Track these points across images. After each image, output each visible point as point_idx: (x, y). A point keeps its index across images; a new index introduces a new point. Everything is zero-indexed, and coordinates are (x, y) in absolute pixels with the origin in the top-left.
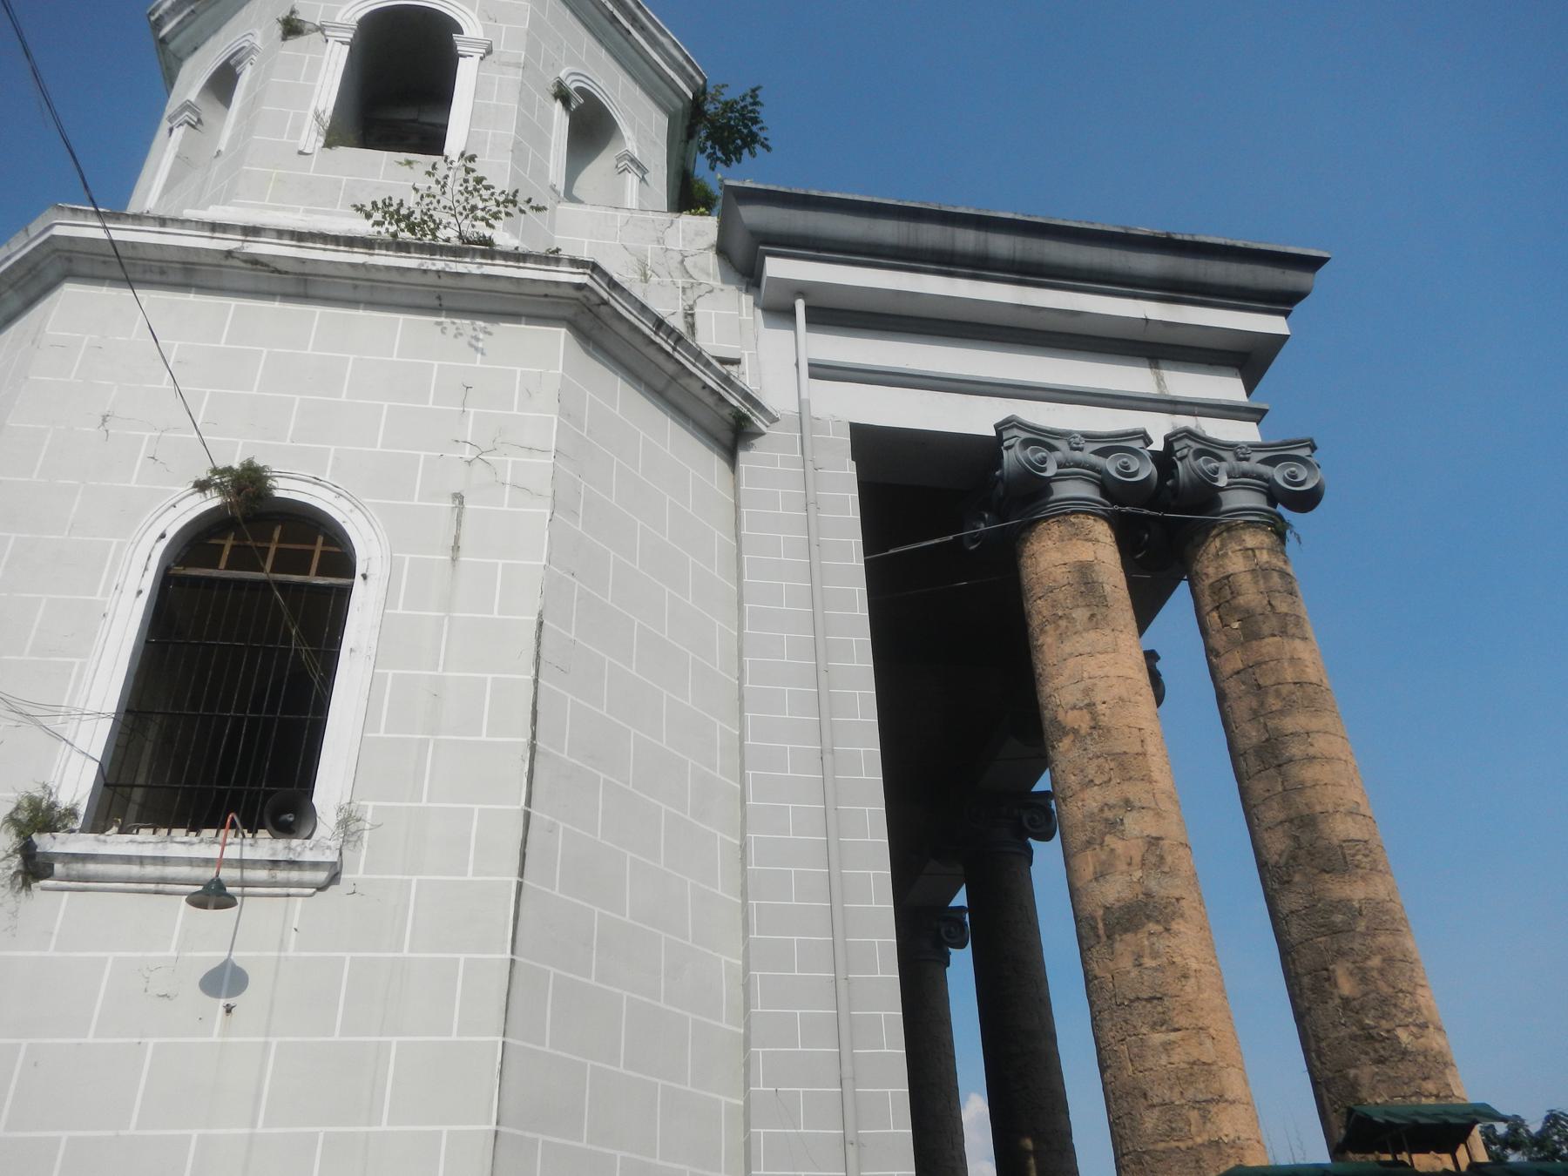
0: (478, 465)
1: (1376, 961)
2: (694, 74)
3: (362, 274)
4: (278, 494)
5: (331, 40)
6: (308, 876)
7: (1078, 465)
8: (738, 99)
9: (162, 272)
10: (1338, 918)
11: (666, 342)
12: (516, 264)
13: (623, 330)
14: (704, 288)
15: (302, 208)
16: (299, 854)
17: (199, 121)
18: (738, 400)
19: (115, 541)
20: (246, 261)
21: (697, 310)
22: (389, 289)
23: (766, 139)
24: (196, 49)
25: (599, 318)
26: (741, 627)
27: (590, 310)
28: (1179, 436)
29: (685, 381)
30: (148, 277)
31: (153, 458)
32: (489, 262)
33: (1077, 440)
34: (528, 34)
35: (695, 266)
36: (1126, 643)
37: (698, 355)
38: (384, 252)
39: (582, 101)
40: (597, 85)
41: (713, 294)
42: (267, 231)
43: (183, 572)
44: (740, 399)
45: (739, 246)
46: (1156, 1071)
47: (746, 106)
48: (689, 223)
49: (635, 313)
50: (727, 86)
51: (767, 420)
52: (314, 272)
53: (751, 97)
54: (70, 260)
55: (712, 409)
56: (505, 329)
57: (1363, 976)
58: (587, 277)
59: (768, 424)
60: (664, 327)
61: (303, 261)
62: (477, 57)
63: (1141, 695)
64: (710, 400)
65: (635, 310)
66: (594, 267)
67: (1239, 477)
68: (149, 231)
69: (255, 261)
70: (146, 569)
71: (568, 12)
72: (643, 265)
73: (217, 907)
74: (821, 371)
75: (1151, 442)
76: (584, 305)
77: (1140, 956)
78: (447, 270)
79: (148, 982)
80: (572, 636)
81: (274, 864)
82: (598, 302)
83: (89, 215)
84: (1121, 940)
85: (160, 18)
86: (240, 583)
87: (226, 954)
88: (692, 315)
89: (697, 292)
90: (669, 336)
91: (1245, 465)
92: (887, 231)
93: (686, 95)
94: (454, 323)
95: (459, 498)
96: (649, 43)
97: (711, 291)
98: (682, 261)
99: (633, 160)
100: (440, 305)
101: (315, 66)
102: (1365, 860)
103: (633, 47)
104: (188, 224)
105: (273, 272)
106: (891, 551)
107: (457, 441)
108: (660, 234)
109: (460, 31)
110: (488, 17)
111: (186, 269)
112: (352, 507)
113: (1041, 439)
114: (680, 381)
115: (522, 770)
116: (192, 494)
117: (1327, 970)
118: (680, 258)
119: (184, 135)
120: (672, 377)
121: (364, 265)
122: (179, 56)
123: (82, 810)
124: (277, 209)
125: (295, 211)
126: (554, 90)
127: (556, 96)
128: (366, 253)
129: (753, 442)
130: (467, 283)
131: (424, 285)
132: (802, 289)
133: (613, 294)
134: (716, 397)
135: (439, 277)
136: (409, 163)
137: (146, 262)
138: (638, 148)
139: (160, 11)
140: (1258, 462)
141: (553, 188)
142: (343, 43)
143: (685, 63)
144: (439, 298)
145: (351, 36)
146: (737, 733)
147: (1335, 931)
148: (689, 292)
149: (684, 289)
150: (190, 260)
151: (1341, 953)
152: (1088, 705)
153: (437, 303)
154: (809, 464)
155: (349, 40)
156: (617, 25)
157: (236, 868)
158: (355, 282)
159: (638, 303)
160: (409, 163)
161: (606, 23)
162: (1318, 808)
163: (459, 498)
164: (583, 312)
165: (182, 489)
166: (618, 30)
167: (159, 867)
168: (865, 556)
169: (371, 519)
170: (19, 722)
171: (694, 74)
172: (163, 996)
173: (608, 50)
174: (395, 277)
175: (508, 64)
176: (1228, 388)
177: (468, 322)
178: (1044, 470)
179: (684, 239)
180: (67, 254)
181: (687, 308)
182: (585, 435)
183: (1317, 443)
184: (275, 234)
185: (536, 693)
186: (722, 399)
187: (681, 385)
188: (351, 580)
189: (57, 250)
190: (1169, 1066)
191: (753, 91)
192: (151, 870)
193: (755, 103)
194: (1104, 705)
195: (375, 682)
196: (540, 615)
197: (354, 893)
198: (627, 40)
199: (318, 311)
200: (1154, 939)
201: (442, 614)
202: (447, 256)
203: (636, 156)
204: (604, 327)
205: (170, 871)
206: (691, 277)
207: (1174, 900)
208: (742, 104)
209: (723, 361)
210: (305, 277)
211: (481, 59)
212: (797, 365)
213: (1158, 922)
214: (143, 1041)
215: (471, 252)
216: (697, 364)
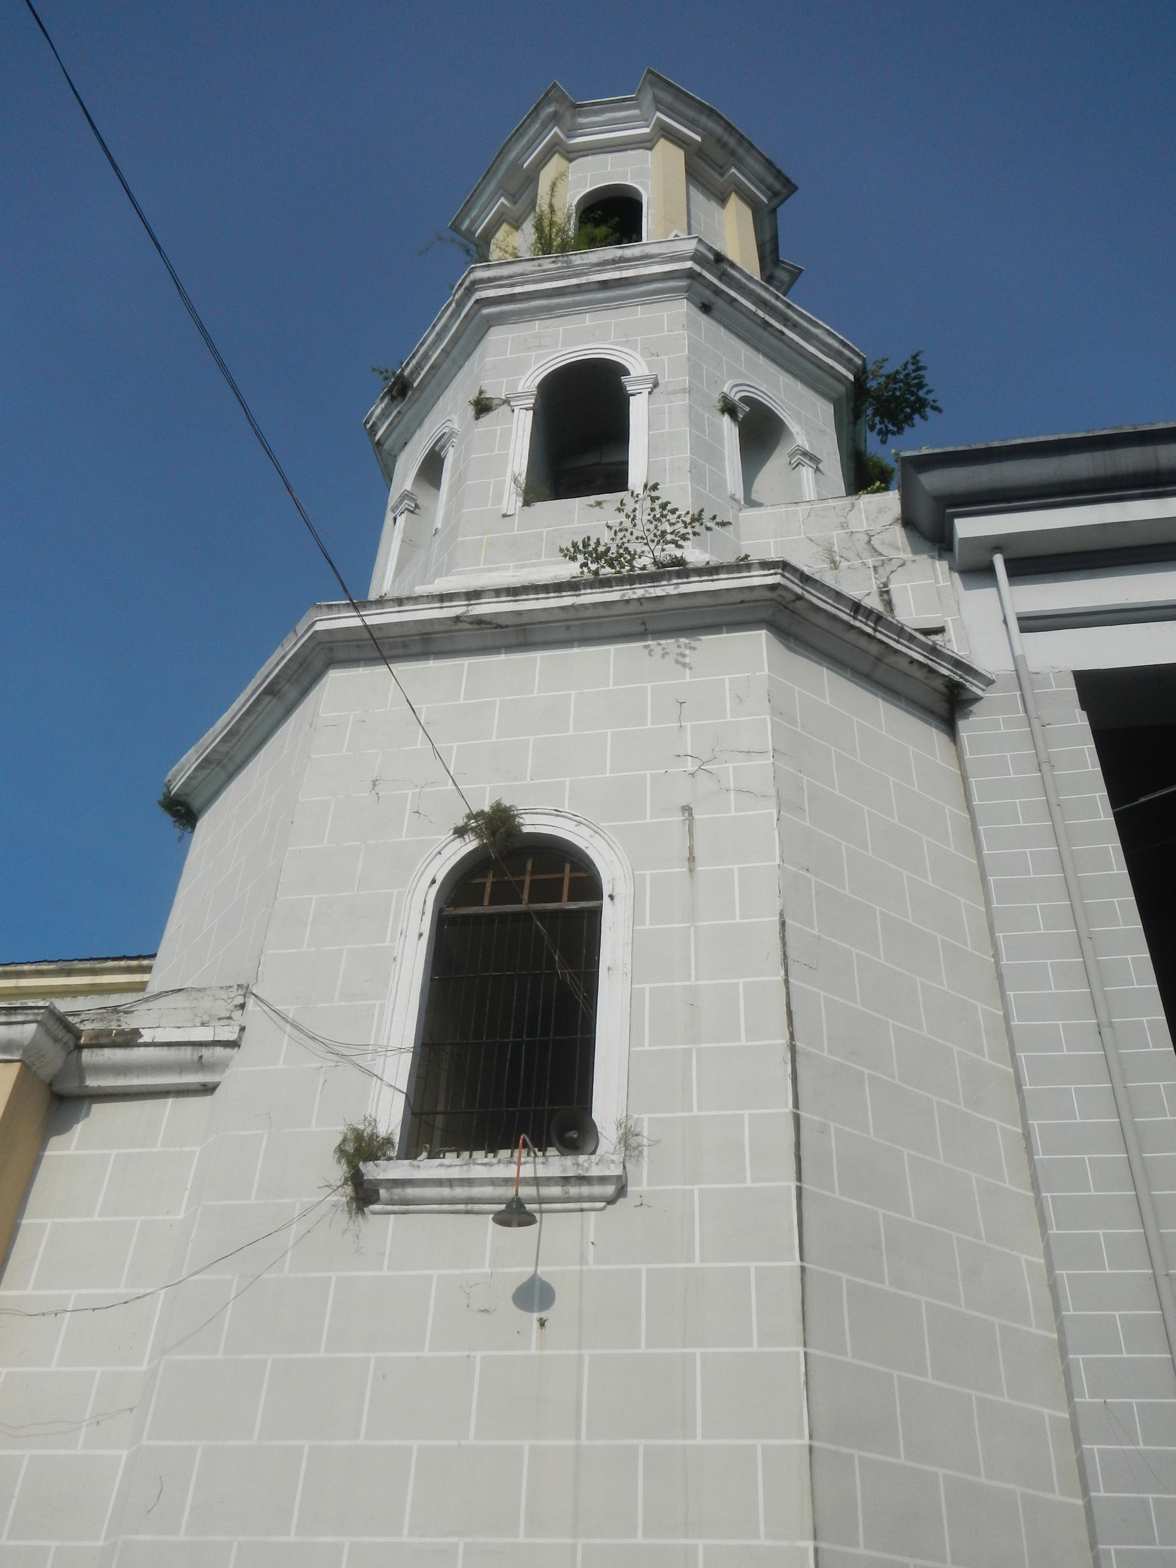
0: (701, 776)
2: (852, 356)
3: (572, 615)
4: (526, 829)
5: (516, 409)
6: (597, 1190)
8: (900, 369)
9: (405, 646)
11: (866, 624)
12: (711, 578)
13: (820, 620)
14: (895, 563)
15: (512, 565)
16: (587, 1169)
17: (417, 506)
18: (948, 669)
19: (395, 891)
20: (471, 623)
21: (891, 586)
23: (934, 401)
24: (406, 444)
25: (798, 614)
26: (988, 902)
27: (786, 608)
29: (891, 659)
30: (394, 652)
31: (417, 812)
32: (685, 580)
34: (689, 361)
35: (883, 543)
37: (900, 631)
38: (589, 591)
39: (747, 409)
40: (760, 391)
41: (905, 567)
42: (486, 593)
43: (453, 912)
44: (950, 667)
45: (924, 516)
47: (908, 375)
48: (869, 502)
49: (831, 602)
50: (887, 360)
51: (982, 684)
52: (530, 621)
53: (913, 364)
54: (331, 649)
55: (923, 683)
56: (708, 640)
58: (779, 576)
59: (984, 687)
60: (861, 611)
61: (519, 613)
62: (646, 392)
64: (920, 674)
66: (785, 566)
68: (390, 612)
69: (480, 622)
70: (423, 913)
71: (722, 329)
72: (830, 552)
73: (520, 1225)
74: (1032, 623)
76: (780, 604)
78: (647, 595)
79: (469, 1298)
80: (816, 932)
81: (566, 1180)
82: (793, 598)
83: (342, 608)
85: (374, 423)
86: (503, 917)
87: (532, 1269)
88: (888, 592)
89: (889, 568)
90: (867, 618)
92: (1080, 465)
93: (846, 378)
94: (660, 644)
95: (687, 810)
97: (902, 565)
98: (869, 542)
99: (805, 454)
100: (646, 630)
101: (507, 434)
103: (788, 345)
104: (420, 599)
105: (496, 628)
106: (1142, 800)
108: (843, 520)
109: (627, 373)
110: (650, 352)
114: (884, 660)
115: (786, 1072)
116: (453, 840)
118: (866, 538)
119: (406, 521)
121: (572, 606)
122: (393, 453)
123: (396, 1139)
124: (491, 570)
125: (507, 568)
126: (719, 405)
127: (723, 411)
128: (573, 595)
129: (971, 708)
130: (668, 604)
132: (998, 544)
133: (807, 588)
134: (925, 670)
135: (641, 604)
136: (599, 504)
137: (391, 640)
138: (808, 440)
139: (374, 419)
141: (733, 498)
142: (527, 409)
143: (841, 348)
144: (644, 623)
145: (533, 401)
146: (1001, 1014)
148: (880, 570)
149: (875, 568)
150: (426, 631)
153: (642, 628)
154: (1036, 724)
155: (532, 405)
156: (770, 329)
157: (533, 1186)
158: (566, 623)
160: (599, 504)
161: (759, 330)
164: (780, 611)
165: (443, 837)
166: (772, 334)
167: (467, 1189)
168: (1113, 808)
169: (610, 842)
170: (337, 1062)
171: (852, 356)
172: (483, 1311)
173: (766, 355)
174: (602, 612)
175: (675, 392)
177: (672, 641)
179: (867, 519)
180: (329, 645)
181: (881, 586)
182: (799, 730)
184: (493, 593)
185: (788, 994)
186: (932, 671)
188: (599, 902)
191: (914, 357)
192: (460, 1192)
193: (918, 369)
195: (634, 998)
196: (781, 915)
197: (642, 1204)
198: (782, 341)
199: (538, 657)
201: (688, 925)
202: (645, 583)
203: (807, 448)
205: (477, 1191)
206: (881, 554)
208: (904, 373)
209: (927, 632)
211: (650, 393)
212: (1005, 622)
214: (472, 1354)
215: (667, 576)
216: (901, 640)
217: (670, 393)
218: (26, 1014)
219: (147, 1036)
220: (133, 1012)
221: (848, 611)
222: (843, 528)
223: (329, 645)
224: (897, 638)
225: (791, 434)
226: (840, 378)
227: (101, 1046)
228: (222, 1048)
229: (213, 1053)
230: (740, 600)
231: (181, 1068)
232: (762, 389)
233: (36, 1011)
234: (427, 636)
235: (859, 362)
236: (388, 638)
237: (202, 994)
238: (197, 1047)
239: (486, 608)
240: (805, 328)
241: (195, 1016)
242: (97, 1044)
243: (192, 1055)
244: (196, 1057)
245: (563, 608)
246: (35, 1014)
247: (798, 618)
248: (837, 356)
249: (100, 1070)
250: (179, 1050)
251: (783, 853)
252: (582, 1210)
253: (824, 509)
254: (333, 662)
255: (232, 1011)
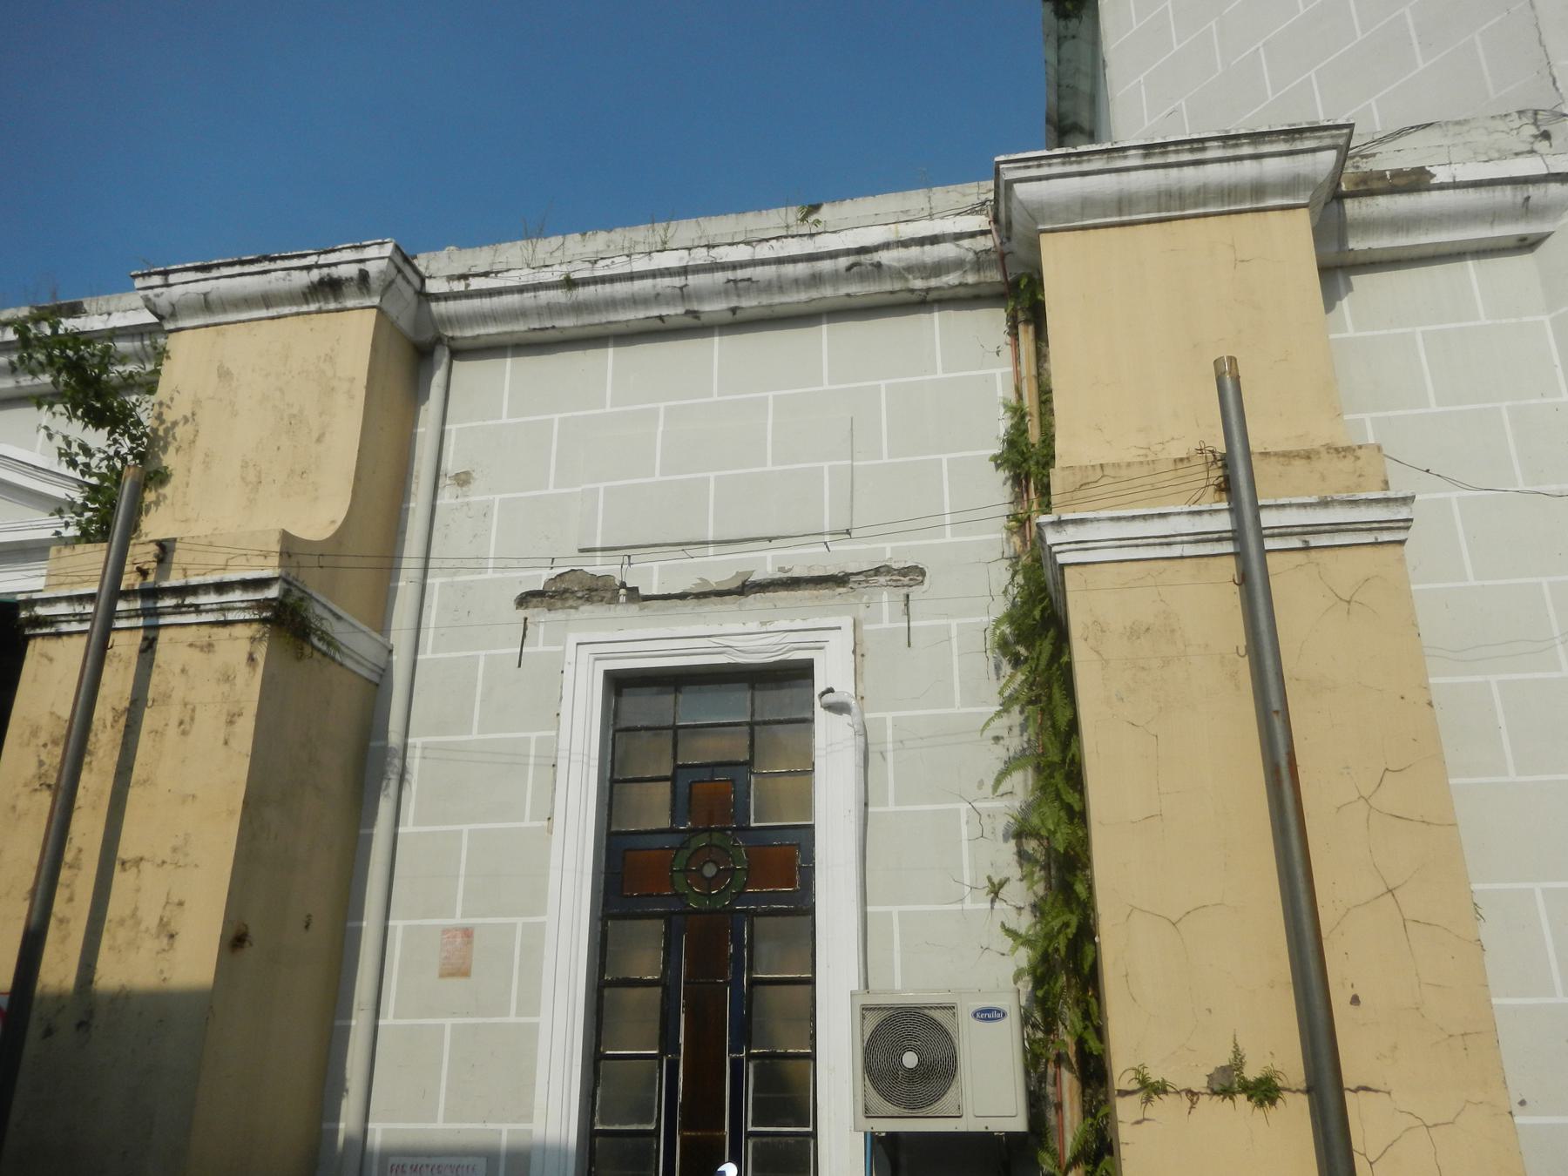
218: (1320, 137)
219: (1442, 175)
220: (1374, 155)
227: (1371, 193)
228: (1558, 185)
229: (1546, 192)
231: (1495, 215)
233: (1334, 132)
237: (1465, 128)
238: (1519, 186)
241: (1475, 153)
242: (1368, 190)
243: (1515, 196)
244: (1520, 199)
246: (1333, 137)
249: (1370, 225)
250: (1494, 192)
255: (1532, 143)
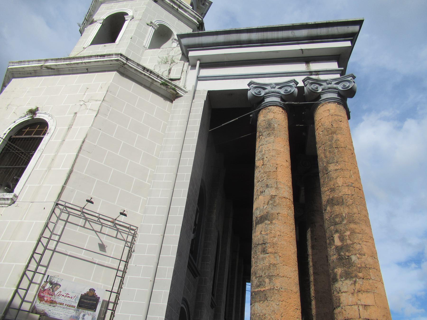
0: (84, 105)
1: (348, 233)
3: (69, 66)
5: (98, 23)
7: (273, 92)
10: (337, 220)
13: (133, 71)
14: (176, 63)
22: (77, 69)
25: (126, 68)
28: (306, 79)
29: (155, 83)
33: (273, 85)
36: (279, 140)
46: (260, 266)
48: (177, 49)
49: (136, 66)
57: (342, 239)
59: (184, 93)
60: (146, 69)
61: (56, 65)
62: (129, 20)
63: (280, 155)
65: (136, 65)
66: (121, 55)
67: (328, 89)
69: (48, 68)
75: (298, 83)
76: (121, 65)
77: (262, 231)
80: (96, 144)
84: (258, 227)
88: (171, 70)
91: (329, 85)
96: (184, 12)
102: (351, 201)
105: (52, 69)
106: (223, 125)
107: (80, 101)
108: (169, 53)
111: (35, 72)
112: (51, 118)
113: (262, 87)
114: (154, 83)
117: (332, 237)
118: (172, 57)
120: (151, 83)
121: (69, 64)
131: (84, 67)
132: (199, 58)
137: (27, 72)
140: (334, 84)
141: (144, 47)
142: (101, 23)
143: (195, 15)
144: (87, 69)
147: (336, 224)
150: (35, 70)
151: (337, 231)
152: (263, 159)
156: (174, 8)
159: (136, 63)
162: (337, 185)
163: (76, 113)
169: (54, 121)
174: (76, 66)
175: (137, 20)
176: (334, 65)
178: (261, 94)
180: (12, 73)
183: (355, 75)
187: (154, 84)
189: (10, 72)
190: (263, 265)
194: (267, 158)
199: (61, 77)
200: (267, 226)
204: (128, 71)
207: (276, 214)
210: (58, 69)
211: (130, 20)
213: (269, 220)
215: (93, 57)
217: (136, 20)
221: (141, 69)
222: (168, 54)
223: (12, 73)
224: (157, 78)
225: (174, 35)
226: (194, 23)
230: (110, 64)
232: (168, 23)
234: (35, 71)
235: (201, 19)
236: (26, 71)
239: (48, 64)
240: (185, 9)
245: (67, 64)
247: (126, 70)
248: (195, 17)
251: (93, 124)
252: (3, 207)
253: (165, 50)
254: (14, 77)
